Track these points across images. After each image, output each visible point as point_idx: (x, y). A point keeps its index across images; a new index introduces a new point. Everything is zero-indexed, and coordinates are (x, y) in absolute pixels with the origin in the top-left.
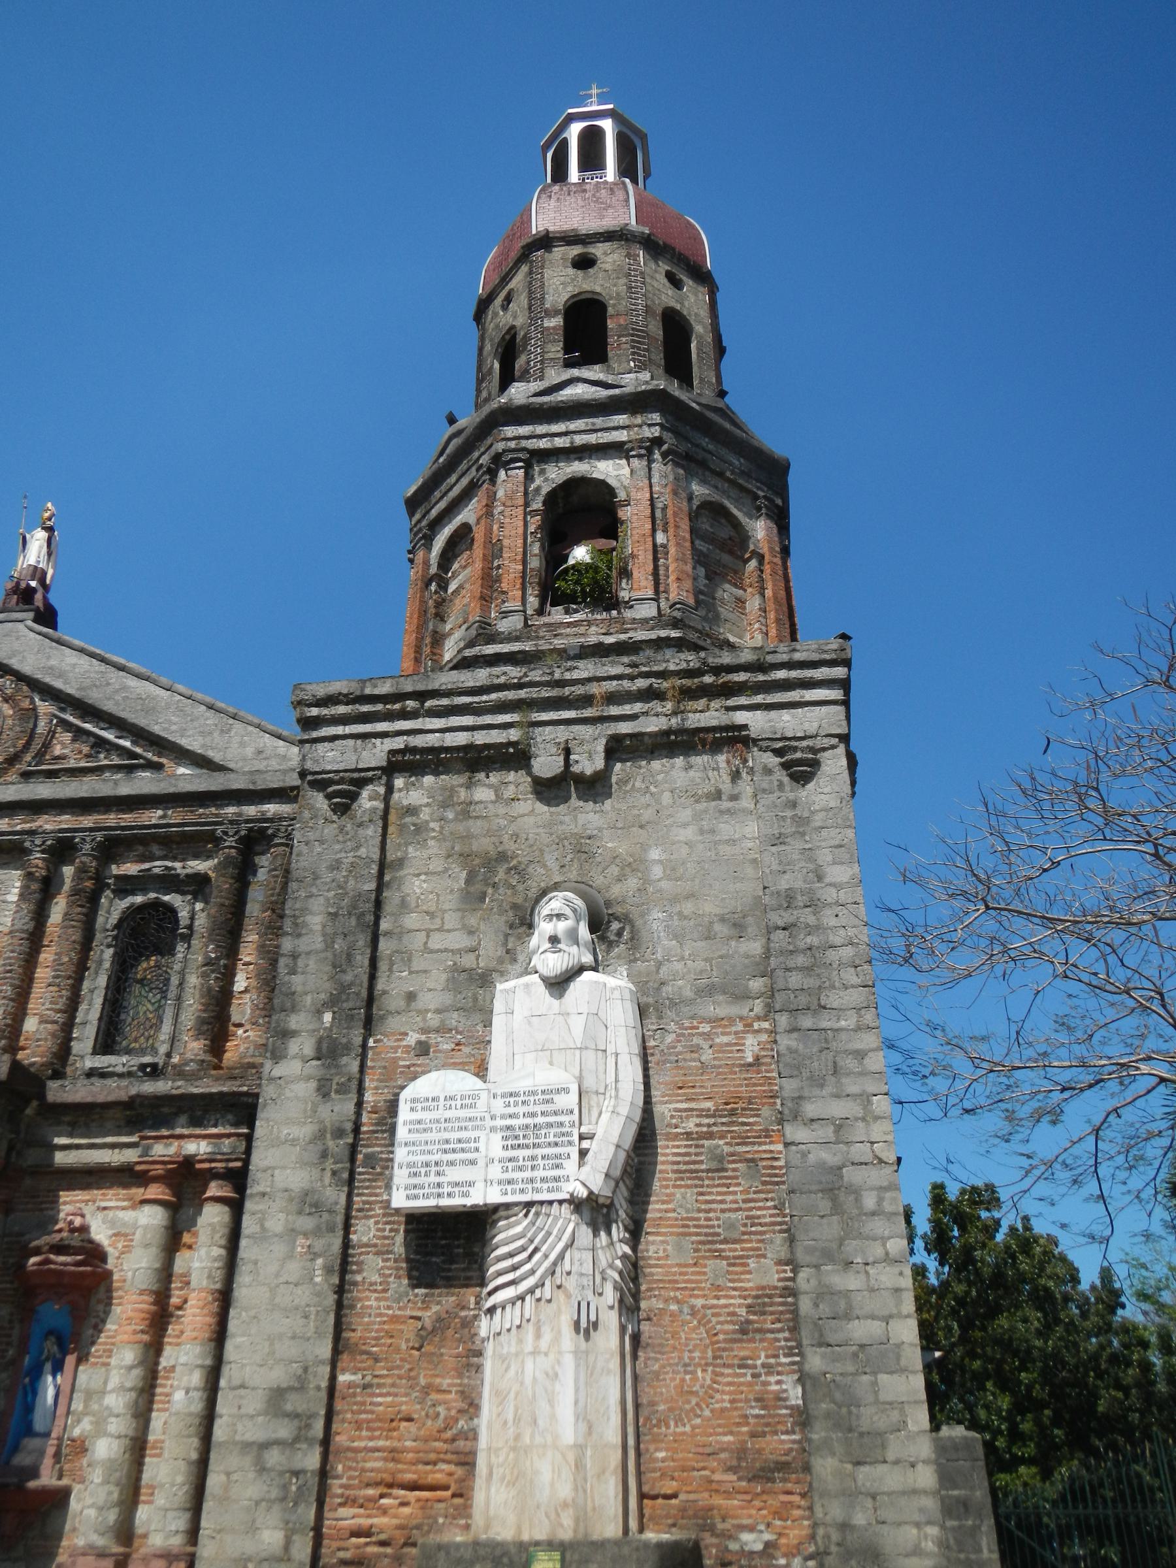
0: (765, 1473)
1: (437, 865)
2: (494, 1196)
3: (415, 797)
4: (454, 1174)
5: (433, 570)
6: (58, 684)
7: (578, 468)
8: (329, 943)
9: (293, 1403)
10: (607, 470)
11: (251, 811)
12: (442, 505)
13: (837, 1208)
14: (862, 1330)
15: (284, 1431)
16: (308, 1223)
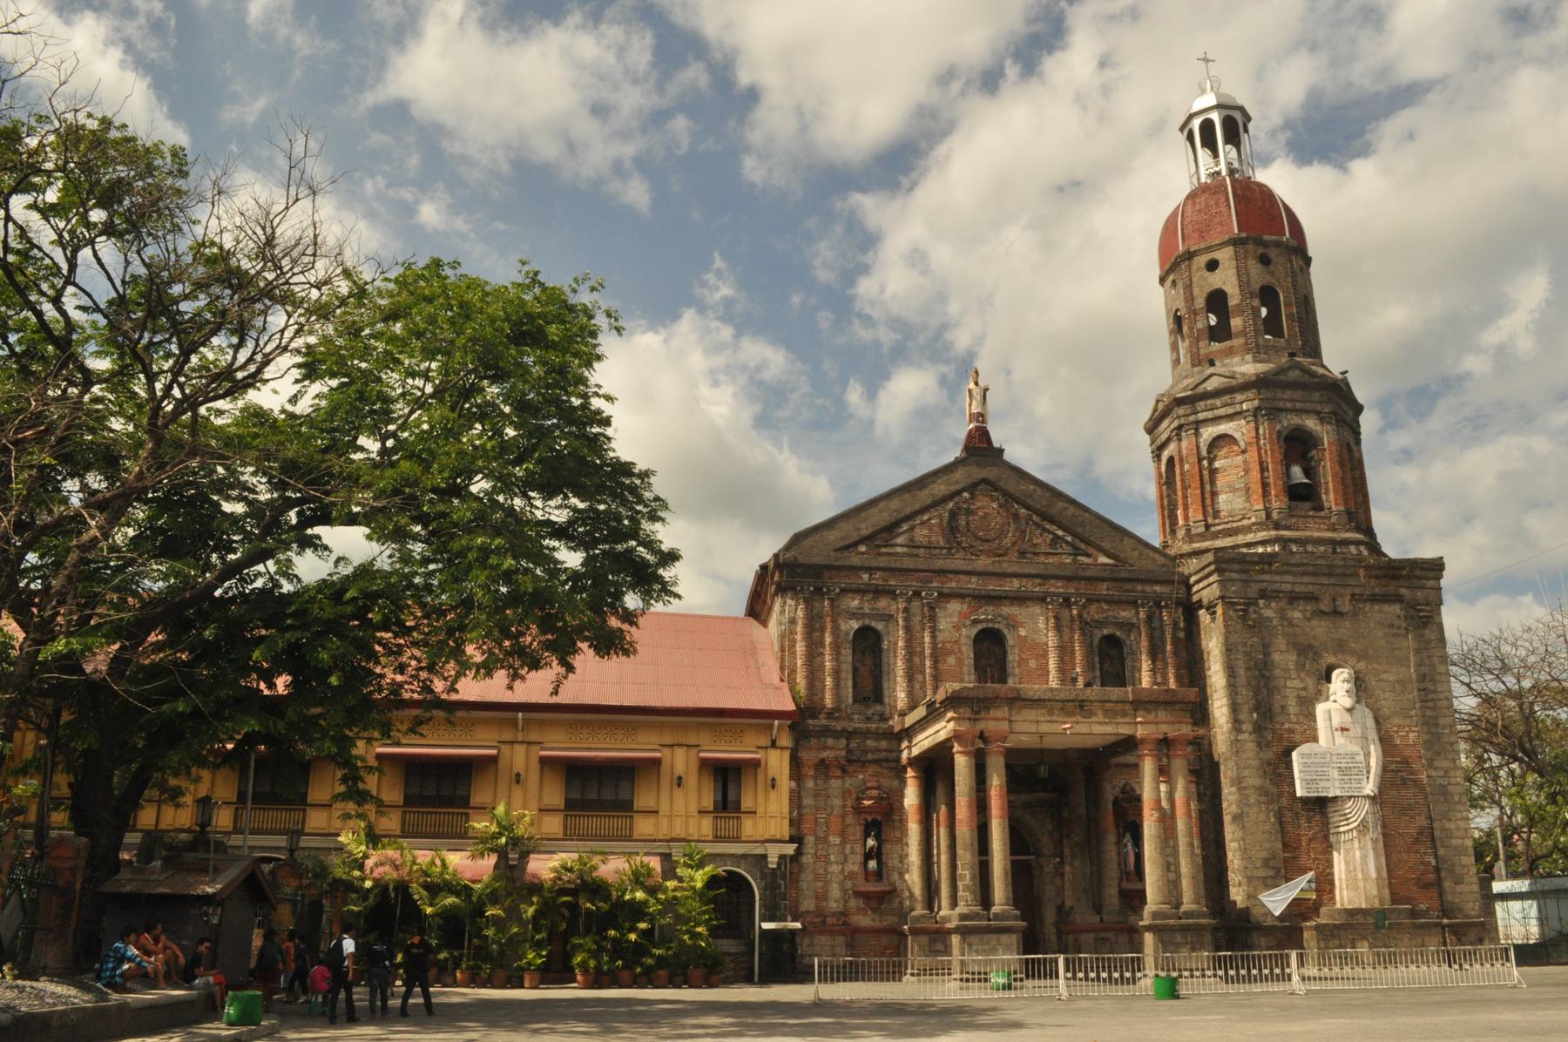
0: (1427, 886)
1: (1283, 647)
2: (1338, 793)
3: (1268, 613)
4: (1322, 784)
5: (1204, 453)
6: (1029, 501)
7: (1296, 420)
8: (1249, 684)
9: (1272, 863)
10: (1311, 423)
11: (1148, 588)
12: (1209, 415)
13: (1446, 800)
14: (1455, 842)
15: (1271, 873)
16: (1263, 799)
